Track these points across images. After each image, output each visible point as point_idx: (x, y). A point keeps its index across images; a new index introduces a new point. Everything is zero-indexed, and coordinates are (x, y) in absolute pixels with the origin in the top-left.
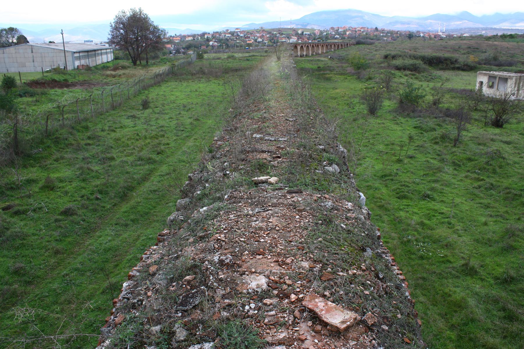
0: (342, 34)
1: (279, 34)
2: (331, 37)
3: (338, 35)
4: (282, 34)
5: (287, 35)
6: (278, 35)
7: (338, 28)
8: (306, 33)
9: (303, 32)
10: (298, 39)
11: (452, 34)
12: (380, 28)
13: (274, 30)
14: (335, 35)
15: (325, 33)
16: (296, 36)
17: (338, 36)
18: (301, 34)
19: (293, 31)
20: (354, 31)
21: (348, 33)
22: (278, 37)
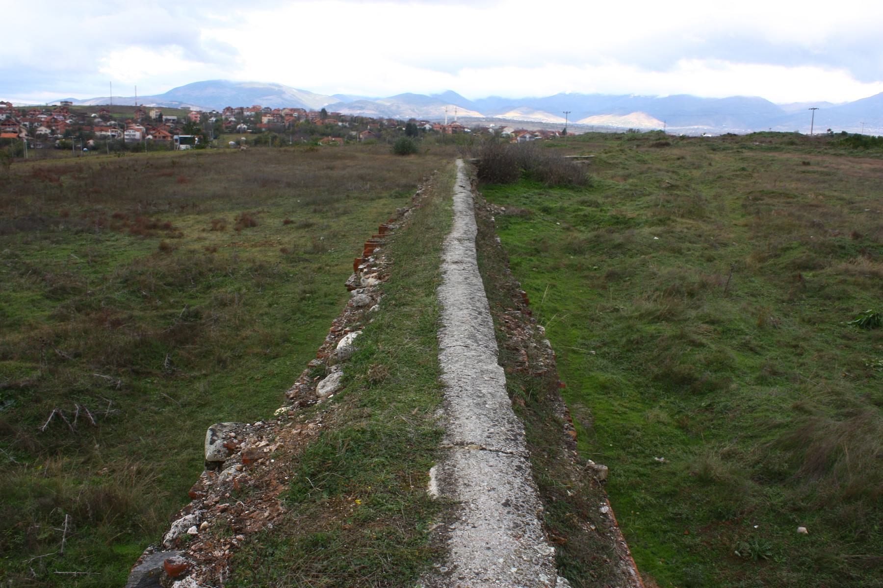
0: (252, 122)
1: (101, 117)
2: (227, 128)
4: (111, 118)
5: (122, 120)
6: (97, 120)
7: (242, 109)
8: (169, 117)
9: (161, 116)
10: (147, 130)
12: (330, 111)
13: (92, 109)
14: (238, 123)
15: (214, 119)
16: (142, 124)
17: (245, 126)
20: (276, 114)
21: (265, 120)
22: (97, 125)
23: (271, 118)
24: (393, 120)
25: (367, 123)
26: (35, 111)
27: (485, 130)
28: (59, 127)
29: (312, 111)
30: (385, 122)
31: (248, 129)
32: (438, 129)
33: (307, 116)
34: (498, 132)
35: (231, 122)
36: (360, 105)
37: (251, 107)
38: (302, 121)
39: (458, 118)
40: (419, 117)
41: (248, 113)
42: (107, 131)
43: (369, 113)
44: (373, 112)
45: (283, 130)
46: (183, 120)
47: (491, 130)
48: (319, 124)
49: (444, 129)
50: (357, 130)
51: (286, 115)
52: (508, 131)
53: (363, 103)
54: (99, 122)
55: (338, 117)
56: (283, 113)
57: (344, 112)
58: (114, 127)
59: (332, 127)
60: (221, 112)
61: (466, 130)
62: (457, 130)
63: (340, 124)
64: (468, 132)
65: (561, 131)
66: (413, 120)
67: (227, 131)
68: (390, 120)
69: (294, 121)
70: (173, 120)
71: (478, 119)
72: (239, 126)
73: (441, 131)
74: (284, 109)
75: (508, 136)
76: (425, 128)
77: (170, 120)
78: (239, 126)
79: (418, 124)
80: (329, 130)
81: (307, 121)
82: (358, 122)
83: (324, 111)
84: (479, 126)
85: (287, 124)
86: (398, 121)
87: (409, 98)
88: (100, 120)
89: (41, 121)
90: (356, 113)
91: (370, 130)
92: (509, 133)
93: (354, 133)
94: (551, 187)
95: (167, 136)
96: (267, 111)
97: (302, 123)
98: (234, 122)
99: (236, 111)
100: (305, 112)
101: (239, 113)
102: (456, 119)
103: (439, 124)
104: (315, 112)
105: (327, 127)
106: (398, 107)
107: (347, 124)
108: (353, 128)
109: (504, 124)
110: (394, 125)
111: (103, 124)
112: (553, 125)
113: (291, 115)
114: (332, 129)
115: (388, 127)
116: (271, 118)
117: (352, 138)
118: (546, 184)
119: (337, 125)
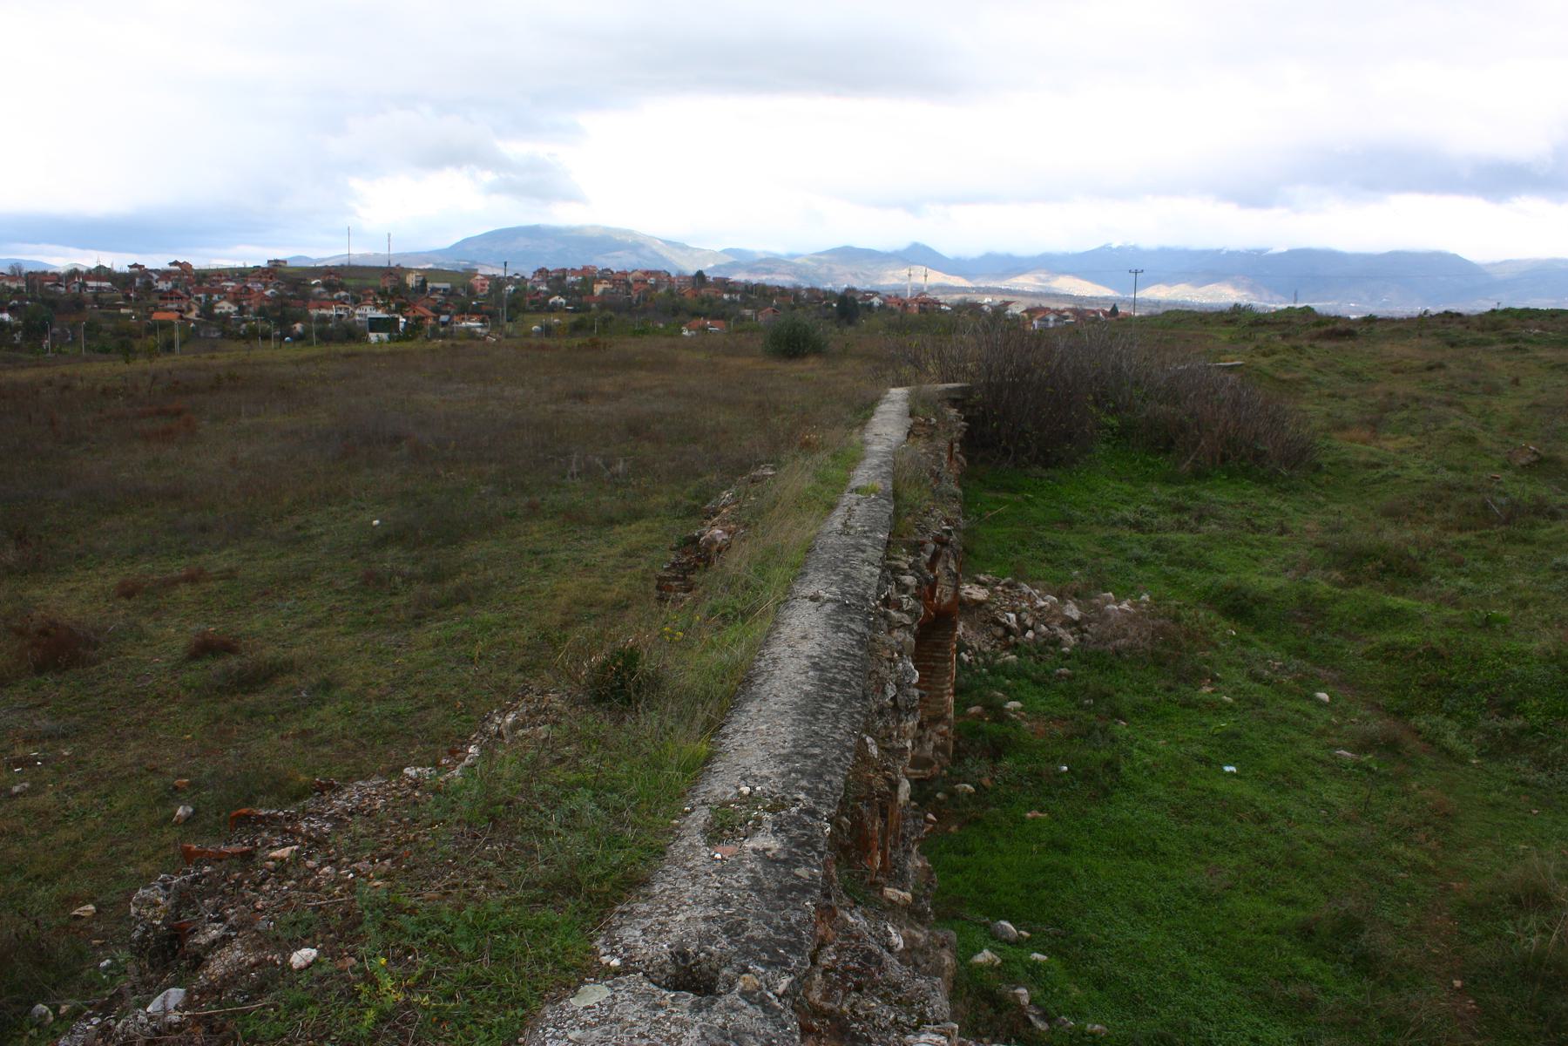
0: (575, 293)
2: (532, 303)
3: (561, 295)
4: (342, 287)
8: (438, 285)
9: (424, 283)
11: (931, 296)
13: (316, 272)
14: (551, 297)
15: (511, 288)
17: (562, 300)
18: (415, 290)
19: (384, 276)
21: (598, 289)
23: (609, 286)
24: (818, 290)
25: (772, 296)
26: (220, 276)
27: (975, 308)
28: (252, 302)
29: (681, 276)
30: (803, 292)
31: (567, 304)
32: (894, 306)
33: (671, 281)
34: (999, 310)
35: (538, 293)
36: (767, 266)
37: (579, 268)
38: (662, 291)
39: (931, 288)
40: (858, 284)
41: (573, 279)
42: (329, 308)
43: (782, 279)
44: (788, 278)
45: (629, 308)
46: (460, 290)
47: (986, 308)
48: (688, 296)
49: (905, 305)
50: (753, 307)
51: (636, 281)
52: (1017, 309)
53: (772, 263)
54: (320, 293)
55: (724, 284)
56: (630, 279)
57: (739, 277)
58: (341, 301)
59: (711, 301)
60: (529, 276)
61: (943, 307)
62: (928, 306)
63: (726, 296)
64: (946, 311)
65: (1108, 310)
66: (850, 290)
67: (532, 308)
68: (811, 290)
69: (647, 291)
70: (445, 290)
71: (964, 290)
72: (551, 301)
73: (899, 309)
74: (633, 271)
75: (1016, 318)
76: (872, 304)
77: (439, 289)
78: (551, 301)
79: (859, 297)
80: (705, 307)
81: (670, 292)
82: (758, 294)
83: (700, 275)
84: (965, 299)
85: (636, 296)
86: (825, 292)
87: (848, 255)
88: (322, 289)
89: (226, 292)
90: (755, 279)
91: (777, 307)
92: (1018, 312)
93: (748, 312)
94: (1199, 475)
95: (427, 317)
96: (606, 275)
97: (660, 295)
98: (546, 292)
99: (554, 275)
100: (669, 275)
101: (557, 278)
102: (925, 290)
103: (897, 296)
104: (686, 277)
105: (703, 302)
106: (830, 269)
107: (738, 297)
108: (746, 303)
109: (1007, 298)
110: (819, 298)
111: (326, 296)
112: (1092, 300)
113: (645, 282)
114: (710, 305)
115: (809, 301)
116: (609, 286)
117: (743, 318)
118: (1186, 467)
119: (722, 298)
